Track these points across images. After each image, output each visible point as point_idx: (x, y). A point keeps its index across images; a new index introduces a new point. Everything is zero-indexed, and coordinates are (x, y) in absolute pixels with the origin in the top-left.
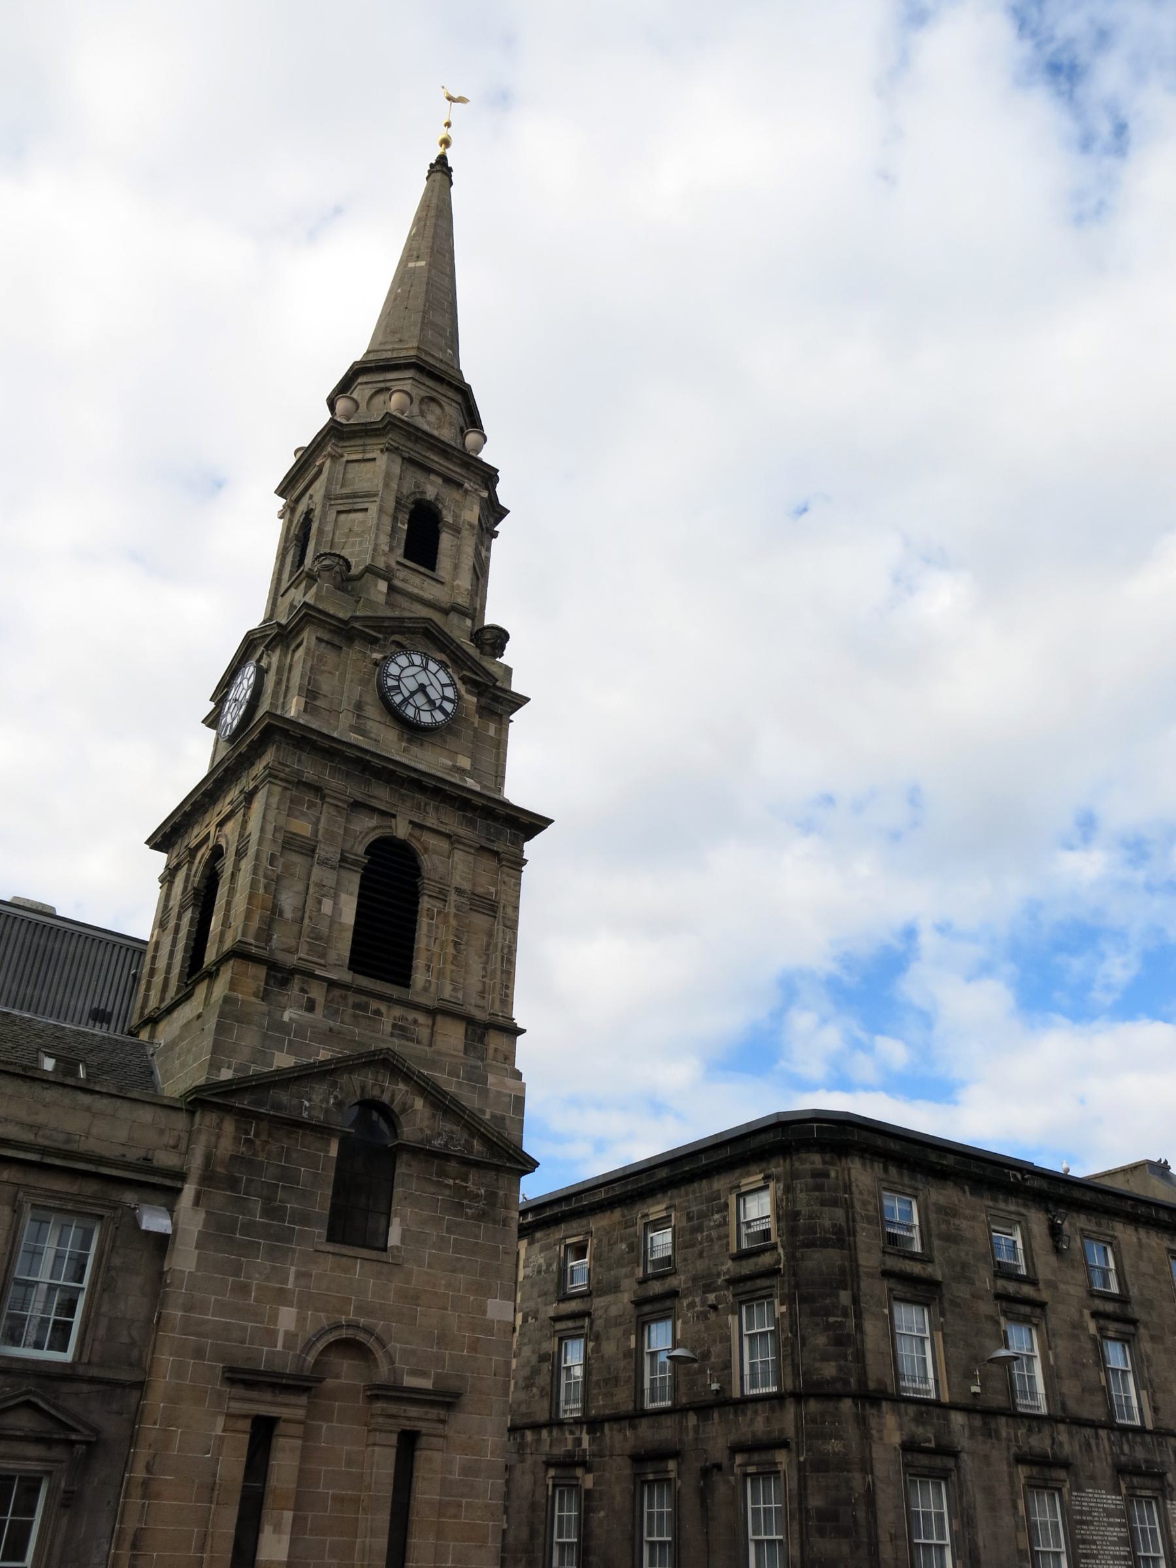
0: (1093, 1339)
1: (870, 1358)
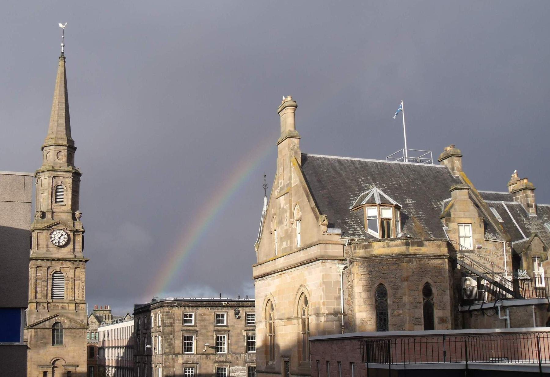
1: (176, 348)
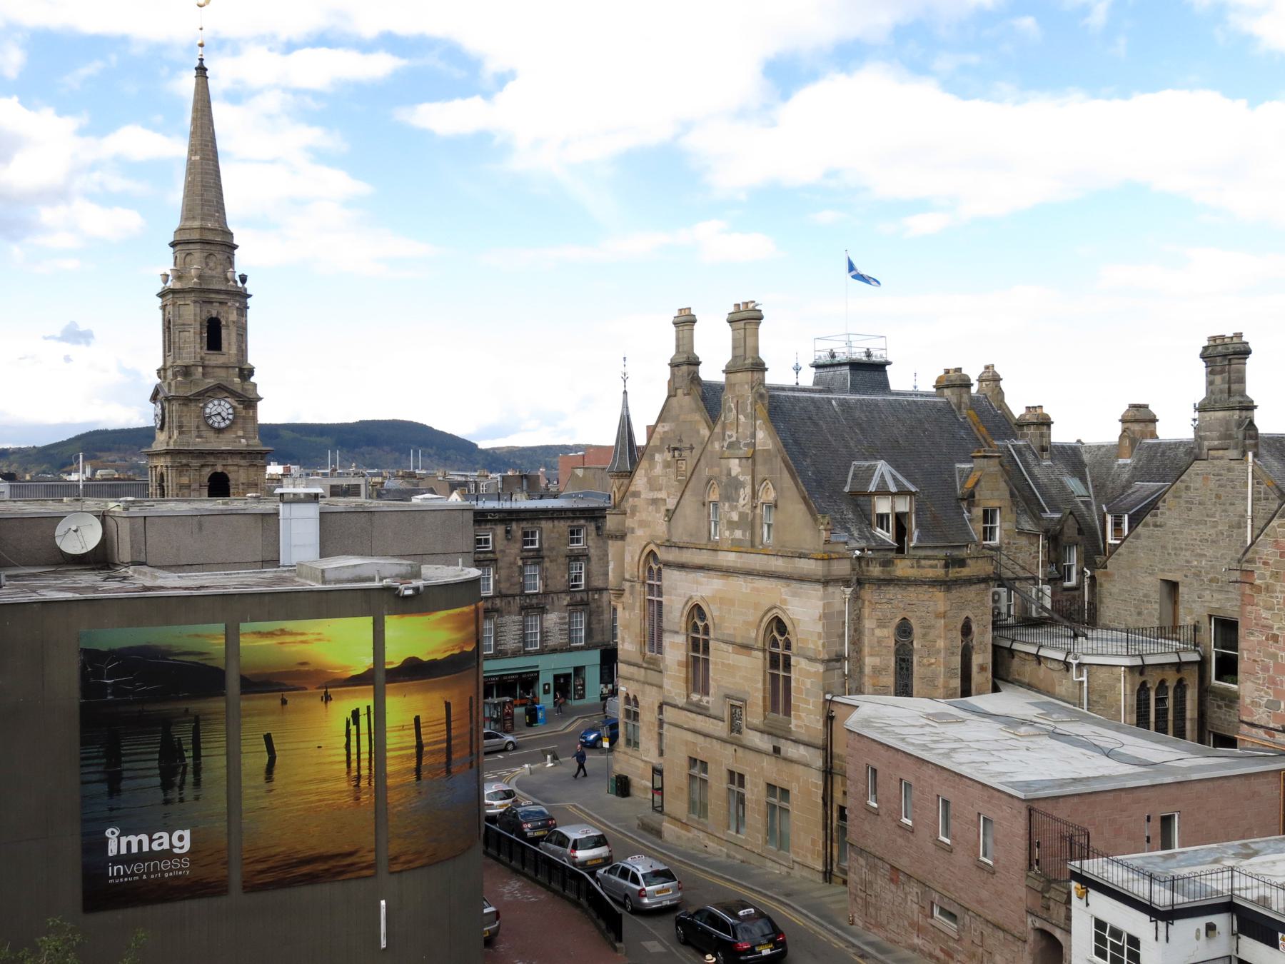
0: (520, 567)
